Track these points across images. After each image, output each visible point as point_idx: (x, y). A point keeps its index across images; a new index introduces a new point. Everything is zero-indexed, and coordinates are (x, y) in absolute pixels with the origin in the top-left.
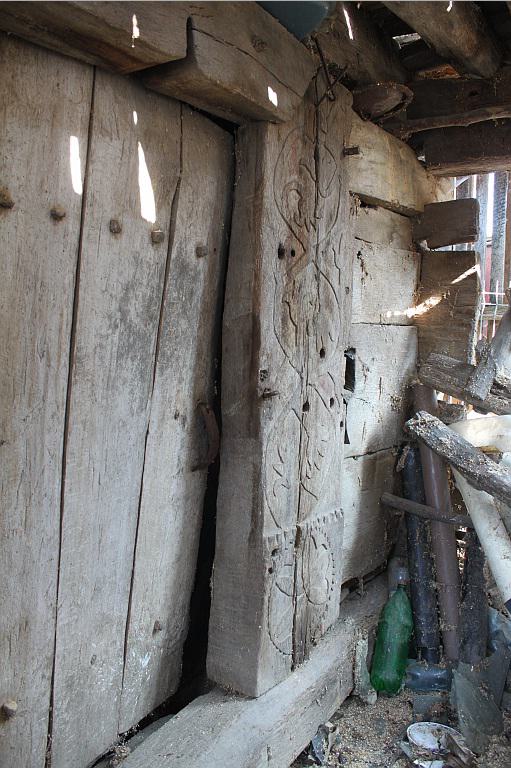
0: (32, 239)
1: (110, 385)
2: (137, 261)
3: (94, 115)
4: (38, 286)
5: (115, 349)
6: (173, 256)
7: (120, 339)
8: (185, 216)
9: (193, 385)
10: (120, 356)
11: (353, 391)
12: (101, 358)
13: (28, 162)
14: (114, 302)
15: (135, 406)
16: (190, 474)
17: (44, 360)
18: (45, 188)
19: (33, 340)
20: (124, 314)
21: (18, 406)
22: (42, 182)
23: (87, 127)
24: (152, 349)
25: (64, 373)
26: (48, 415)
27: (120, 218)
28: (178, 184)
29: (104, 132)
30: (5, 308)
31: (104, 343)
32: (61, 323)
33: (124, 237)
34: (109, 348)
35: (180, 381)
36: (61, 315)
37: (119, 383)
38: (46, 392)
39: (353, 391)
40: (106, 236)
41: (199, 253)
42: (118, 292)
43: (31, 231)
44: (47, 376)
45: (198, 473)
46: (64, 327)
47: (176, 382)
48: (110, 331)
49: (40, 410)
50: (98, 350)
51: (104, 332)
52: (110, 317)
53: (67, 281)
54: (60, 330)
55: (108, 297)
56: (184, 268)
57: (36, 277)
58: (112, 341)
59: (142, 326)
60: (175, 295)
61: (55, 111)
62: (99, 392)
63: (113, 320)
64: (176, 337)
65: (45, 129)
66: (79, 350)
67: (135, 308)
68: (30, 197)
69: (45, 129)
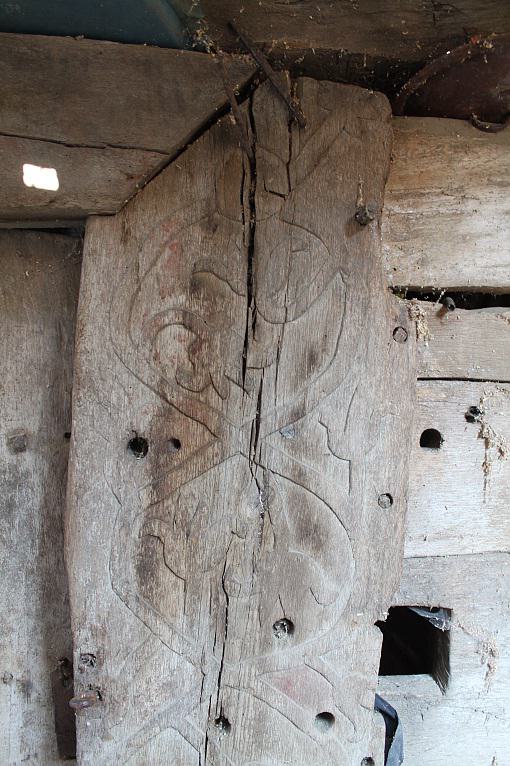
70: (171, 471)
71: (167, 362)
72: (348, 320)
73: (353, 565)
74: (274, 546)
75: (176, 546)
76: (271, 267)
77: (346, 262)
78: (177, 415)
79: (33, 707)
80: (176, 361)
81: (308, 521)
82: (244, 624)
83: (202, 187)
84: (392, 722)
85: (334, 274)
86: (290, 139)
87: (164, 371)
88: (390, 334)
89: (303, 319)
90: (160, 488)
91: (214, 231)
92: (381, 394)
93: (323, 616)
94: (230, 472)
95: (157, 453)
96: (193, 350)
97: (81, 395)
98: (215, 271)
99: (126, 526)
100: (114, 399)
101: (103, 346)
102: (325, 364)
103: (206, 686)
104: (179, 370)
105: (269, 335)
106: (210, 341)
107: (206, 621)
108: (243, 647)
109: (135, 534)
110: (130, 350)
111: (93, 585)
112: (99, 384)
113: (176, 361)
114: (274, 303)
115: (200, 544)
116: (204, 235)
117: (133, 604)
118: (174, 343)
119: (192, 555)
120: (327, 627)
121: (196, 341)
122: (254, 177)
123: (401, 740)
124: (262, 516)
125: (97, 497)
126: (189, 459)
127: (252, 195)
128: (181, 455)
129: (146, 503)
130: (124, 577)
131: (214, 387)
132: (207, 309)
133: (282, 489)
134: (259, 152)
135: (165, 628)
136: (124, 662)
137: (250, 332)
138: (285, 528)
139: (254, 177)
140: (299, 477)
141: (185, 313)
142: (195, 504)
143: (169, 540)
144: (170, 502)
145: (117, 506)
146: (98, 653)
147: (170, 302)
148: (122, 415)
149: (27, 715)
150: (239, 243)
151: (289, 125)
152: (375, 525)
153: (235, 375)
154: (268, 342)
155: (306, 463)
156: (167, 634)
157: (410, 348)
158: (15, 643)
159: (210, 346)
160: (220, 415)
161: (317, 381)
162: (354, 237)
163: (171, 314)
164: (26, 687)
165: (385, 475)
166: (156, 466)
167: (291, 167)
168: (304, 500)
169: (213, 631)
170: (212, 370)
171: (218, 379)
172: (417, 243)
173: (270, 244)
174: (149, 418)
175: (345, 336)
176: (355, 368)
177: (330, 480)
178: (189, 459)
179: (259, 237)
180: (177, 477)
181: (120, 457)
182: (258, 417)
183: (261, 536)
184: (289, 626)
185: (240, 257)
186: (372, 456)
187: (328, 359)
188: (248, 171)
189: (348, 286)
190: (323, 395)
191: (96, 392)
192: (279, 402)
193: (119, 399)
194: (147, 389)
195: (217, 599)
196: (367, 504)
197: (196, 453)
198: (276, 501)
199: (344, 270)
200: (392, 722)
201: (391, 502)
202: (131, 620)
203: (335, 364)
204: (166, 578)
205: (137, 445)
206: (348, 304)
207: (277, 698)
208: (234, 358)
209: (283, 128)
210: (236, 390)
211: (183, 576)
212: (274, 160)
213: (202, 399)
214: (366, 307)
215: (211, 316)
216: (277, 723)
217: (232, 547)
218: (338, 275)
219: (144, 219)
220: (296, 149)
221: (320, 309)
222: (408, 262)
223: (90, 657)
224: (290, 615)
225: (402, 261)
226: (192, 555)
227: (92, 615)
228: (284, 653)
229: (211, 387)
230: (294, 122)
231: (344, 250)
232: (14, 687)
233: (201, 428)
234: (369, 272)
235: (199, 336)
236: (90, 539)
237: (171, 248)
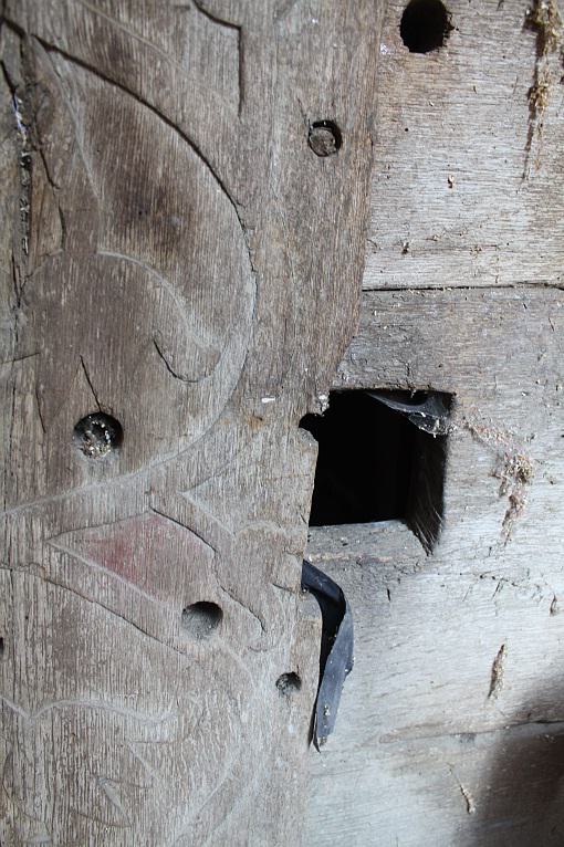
11: (429, 548)
39: (429, 548)
73: (250, 288)
81: (142, 179)
84: (333, 608)
93: (187, 406)
120: (196, 429)
123: (349, 638)
124: (27, 164)
138: (85, 195)
168: (131, 125)
198: (60, 125)
200: (333, 608)
207: (98, 582)
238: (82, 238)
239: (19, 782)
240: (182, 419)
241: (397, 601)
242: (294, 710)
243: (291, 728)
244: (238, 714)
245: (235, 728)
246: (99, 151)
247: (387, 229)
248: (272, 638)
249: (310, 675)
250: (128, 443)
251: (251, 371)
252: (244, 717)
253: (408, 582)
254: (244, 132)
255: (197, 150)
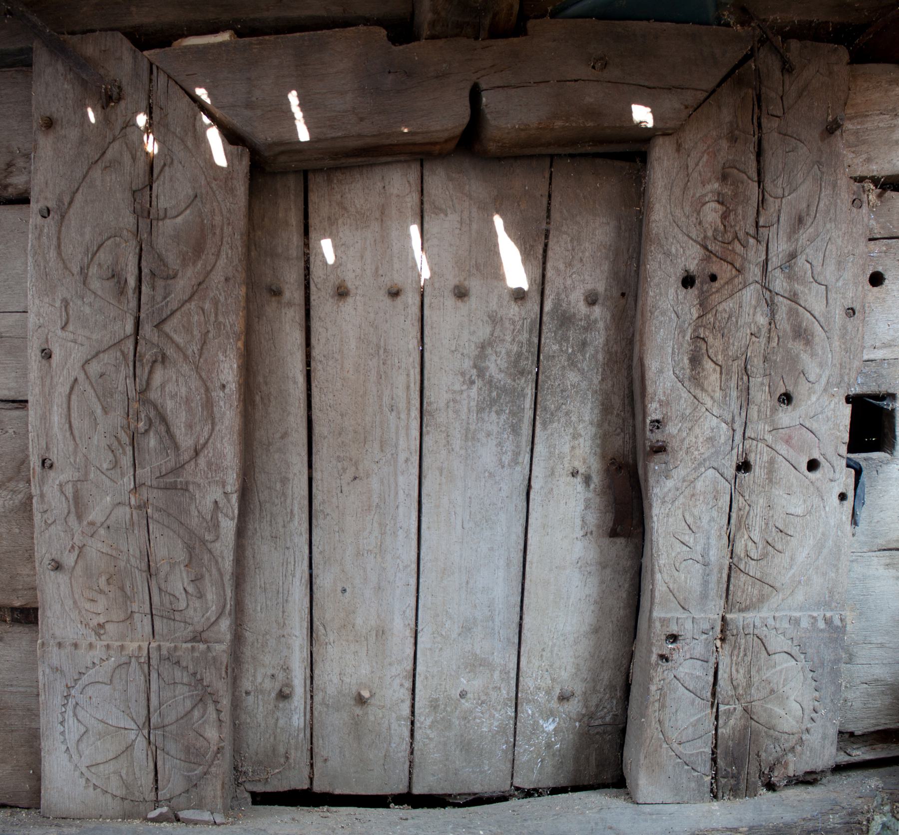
0: (372, 315)
1: (470, 436)
2: (494, 319)
3: (425, 200)
4: (381, 351)
5: (473, 404)
6: (548, 307)
7: (479, 394)
8: (562, 266)
9: (598, 441)
10: (480, 410)
12: (456, 412)
13: (362, 257)
14: (467, 360)
15: (506, 459)
16: (607, 541)
17: (394, 414)
18: (381, 272)
19: (380, 397)
20: (481, 371)
21: (370, 450)
22: (377, 269)
23: (418, 211)
24: (528, 403)
25: (415, 424)
26: (402, 457)
27: (466, 283)
28: (547, 237)
29: (438, 210)
30: (351, 372)
31: (458, 398)
32: (408, 382)
33: (473, 301)
34: (465, 402)
35: (576, 436)
36: (408, 375)
37: (481, 435)
38: (397, 439)
40: (450, 301)
41: (592, 300)
42: (472, 350)
43: (370, 310)
44: (397, 427)
45: (620, 541)
46: (412, 385)
47: (569, 437)
48: (465, 387)
49: (392, 454)
50: (451, 404)
51: (457, 387)
52: (463, 374)
53: (411, 346)
54: (408, 387)
55: (459, 356)
56: (565, 320)
57: (378, 347)
58: (469, 396)
59: (509, 381)
60: (556, 347)
61: (383, 210)
62: (457, 443)
63: (467, 377)
64: (562, 391)
65: (375, 226)
66: (430, 404)
67: (495, 366)
68: (367, 283)
69: (375, 226)
70: (711, 295)
71: (707, 225)
72: (823, 194)
73: (830, 356)
74: (778, 344)
75: (715, 343)
76: (772, 162)
77: (821, 158)
78: (714, 259)
79: (591, 495)
80: (713, 225)
81: (800, 327)
82: (761, 396)
83: (726, 116)
84: (858, 473)
85: (814, 165)
86: (783, 81)
87: (705, 232)
88: (850, 204)
89: (794, 195)
90: (704, 305)
91: (736, 142)
92: (845, 242)
93: (811, 391)
94: (750, 295)
95: (702, 283)
96: (724, 217)
97: (653, 248)
98: (738, 166)
99: (683, 332)
100: (673, 250)
101: (666, 217)
102: (809, 224)
103: (736, 438)
104: (715, 230)
105: (772, 205)
106: (735, 210)
107: (734, 394)
108: (759, 411)
109: (688, 337)
110: (684, 219)
111: (661, 371)
112: (664, 242)
113: (713, 225)
114: (775, 186)
115: (731, 341)
116: (729, 144)
117: (687, 384)
118: (712, 214)
119: (725, 350)
121: (726, 211)
122: (760, 107)
123: (864, 485)
125: (663, 313)
126: (723, 286)
127: (759, 118)
128: (717, 284)
129: (695, 316)
130: (681, 365)
131: (738, 240)
132: (733, 191)
133: (783, 305)
134: (763, 90)
135: (709, 399)
136: (680, 424)
137: (760, 205)
138: (785, 331)
139: (760, 107)
140: (794, 298)
141: (719, 194)
142: (727, 316)
143: (710, 340)
144: (710, 315)
145: (676, 319)
146: (663, 418)
147: (709, 187)
148: (679, 261)
149: (587, 500)
150: (752, 149)
151: (782, 72)
152: (844, 327)
153: (752, 231)
154: (772, 210)
155: (798, 288)
156: (709, 403)
157: (864, 211)
158: (582, 446)
159: (735, 214)
160: (742, 257)
161: (804, 236)
162: (826, 142)
163: (710, 195)
164: (587, 479)
165: (850, 294)
166: (702, 292)
167: (784, 98)
168: (797, 312)
169: (739, 401)
170: (737, 228)
171: (741, 235)
172: (864, 148)
173: (771, 149)
174: (696, 262)
175: (821, 205)
176: (828, 226)
177: (813, 299)
178: (723, 286)
179: (765, 145)
180: (716, 298)
181: (678, 287)
182: (767, 260)
183: (769, 337)
184: (787, 398)
185: (753, 157)
186: (840, 284)
187: (811, 220)
188: (756, 103)
189: (822, 173)
190: (808, 243)
191: (662, 246)
192: (780, 247)
193: (677, 250)
194: (694, 244)
195: (742, 379)
196: (838, 314)
197: (727, 283)
198: (779, 313)
199: (819, 163)
200: (858, 473)
201: (854, 313)
202: (685, 394)
203: (815, 223)
204: (709, 365)
205: (688, 281)
206: (823, 184)
207: (782, 448)
208: (751, 220)
209: (778, 74)
210: (752, 241)
211: (720, 363)
212: (773, 95)
213: (730, 248)
214: (834, 186)
215: (736, 195)
216: (783, 467)
217: (751, 344)
218: (816, 167)
219: (690, 138)
220: (787, 87)
221: (804, 189)
222: (859, 160)
223: (657, 424)
224: (790, 389)
225: (854, 160)
226: (725, 350)
227: (660, 391)
228: (786, 417)
229: (736, 240)
230: (787, 68)
231: (820, 150)
232: (579, 479)
233: (730, 267)
234: (836, 164)
235: (728, 208)
236: (659, 340)
237: (708, 154)
238: (784, 342)
239: (750, 524)
240: (809, 395)
241: (881, 476)
242: (845, 509)
243: (844, 517)
244: (824, 507)
245: (823, 513)
246: (789, 319)
247: (869, 342)
248: (837, 475)
249: (851, 494)
250: (794, 402)
251: (831, 380)
252: (827, 509)
253: (885, 467)
254: (828, 312)
255: (815, 318)
